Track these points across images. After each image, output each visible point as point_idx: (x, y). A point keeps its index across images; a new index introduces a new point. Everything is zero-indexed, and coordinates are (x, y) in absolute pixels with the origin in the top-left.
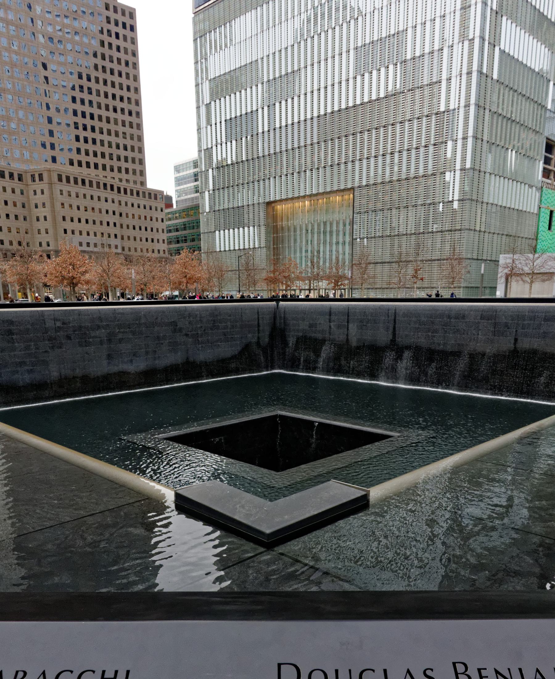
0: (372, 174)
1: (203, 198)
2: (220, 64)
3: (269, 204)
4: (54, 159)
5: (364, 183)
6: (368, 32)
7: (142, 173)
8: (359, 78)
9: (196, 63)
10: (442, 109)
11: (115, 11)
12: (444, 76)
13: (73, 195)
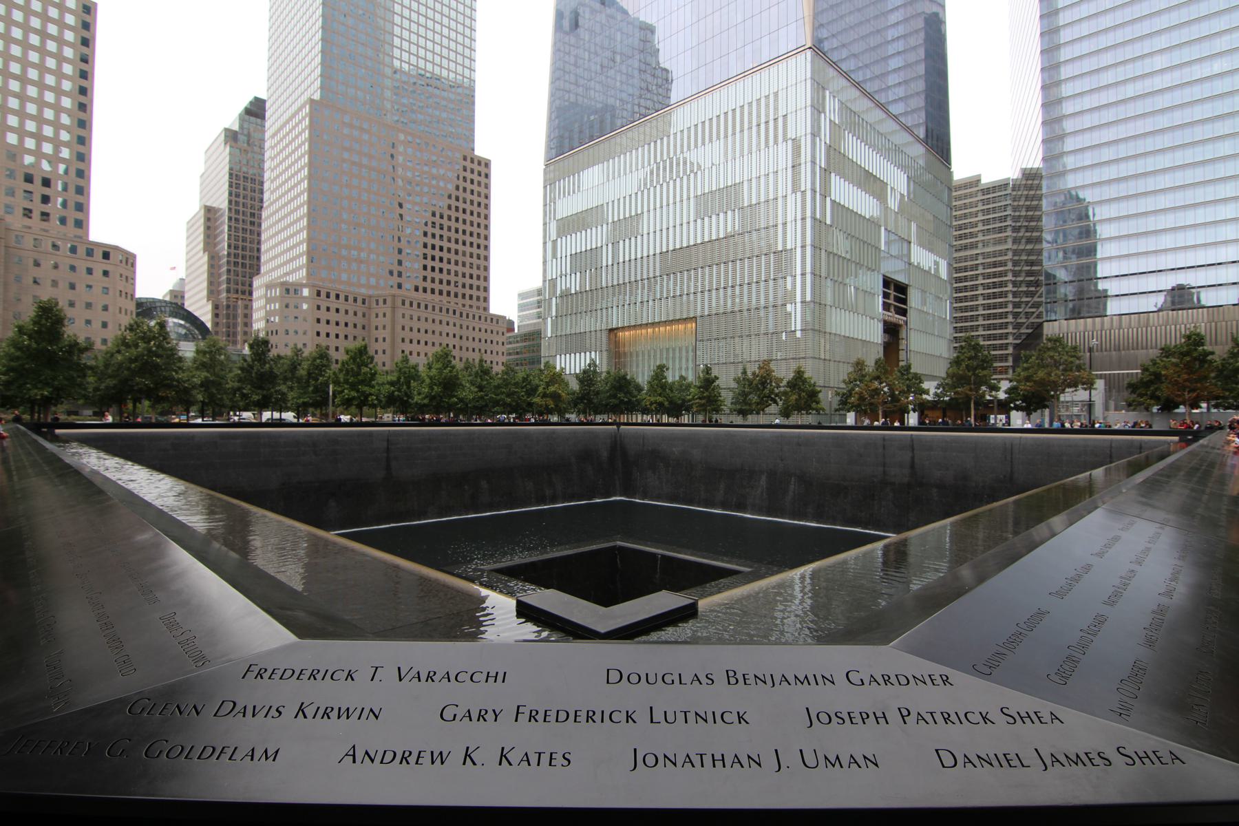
0: (714, 305)
1: (545, 324)
2: (568, 207)
3: (611, 330)
4: (400, 286)
6: (709, 183)
7: (486, 300)
8: (699, 221)
9: (545, 205)
10: (780, 248)
11: (472, 161)
12: (780, 221)
13: (415, 318)
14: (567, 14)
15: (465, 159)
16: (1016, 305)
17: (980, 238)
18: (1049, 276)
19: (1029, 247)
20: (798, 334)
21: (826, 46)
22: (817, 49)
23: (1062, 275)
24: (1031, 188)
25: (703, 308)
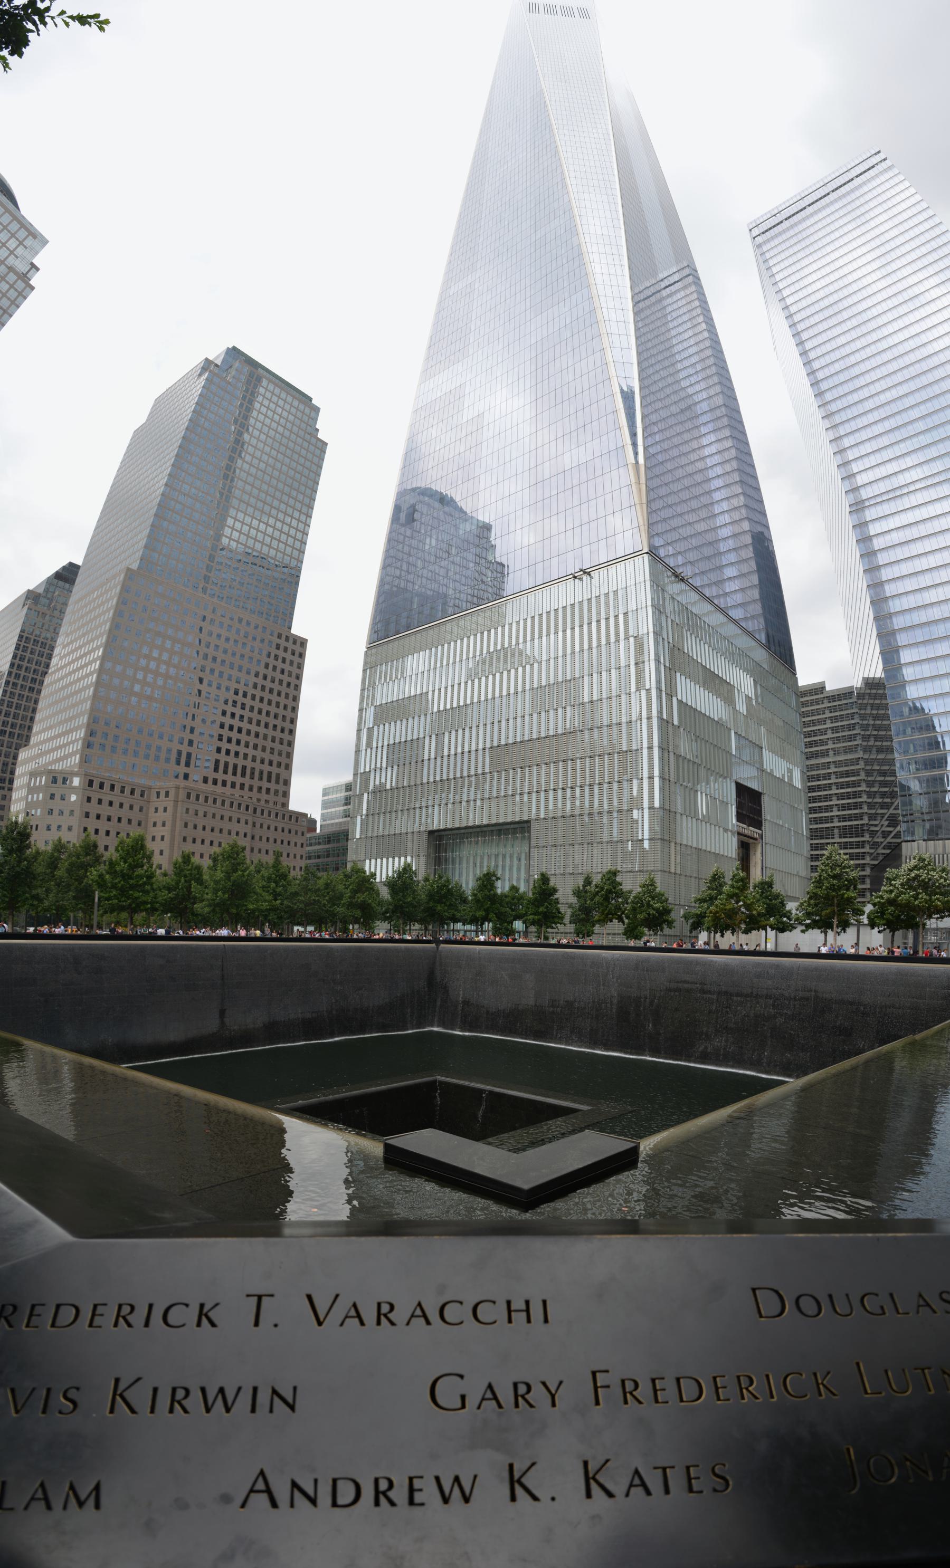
2: (387, 693)
3: (431, 833)
5: (542, 816)
9: (363, 690)
11: (287, 639)
14: (404, 508)
15: (279, 636)
17: (831, 746)
18: (904, 788)
19: (881, 756)
20: (646, 845)
21: (662, 552)
22: (653, 553)
23: (915, 786)
24: (875, 697)
25: (538, 810)
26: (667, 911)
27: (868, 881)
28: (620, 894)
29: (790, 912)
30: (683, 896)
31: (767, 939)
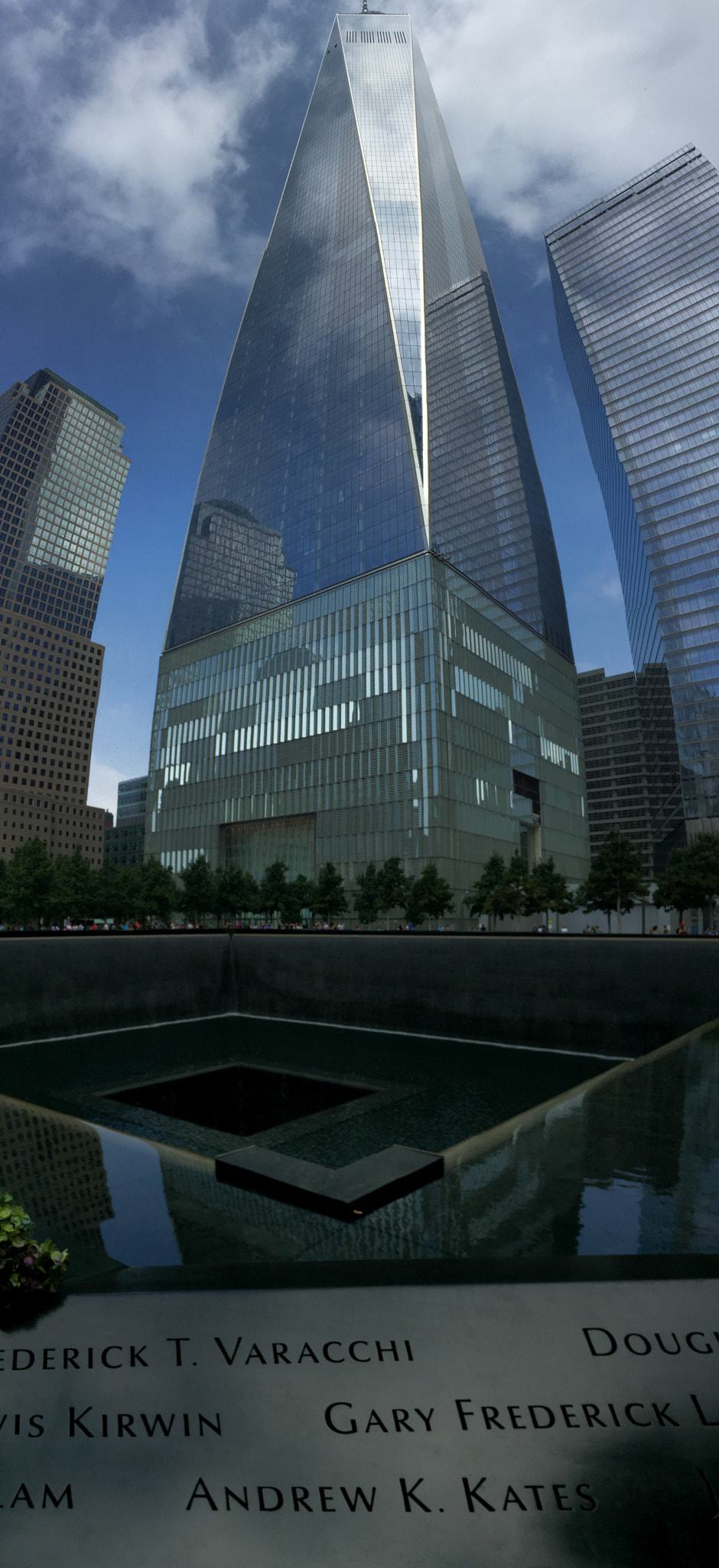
2: (181, 696)
3: (222, 826)
16: (653, 802)
17: (609, 732)
18: (686, 771)
20: (426, 832)
25: (323, 803)
26: (449, 897)
27: (651, 859)
28: (403, 880)
29: (571, 894)
30: (462, 880)
31: (551, 921)
